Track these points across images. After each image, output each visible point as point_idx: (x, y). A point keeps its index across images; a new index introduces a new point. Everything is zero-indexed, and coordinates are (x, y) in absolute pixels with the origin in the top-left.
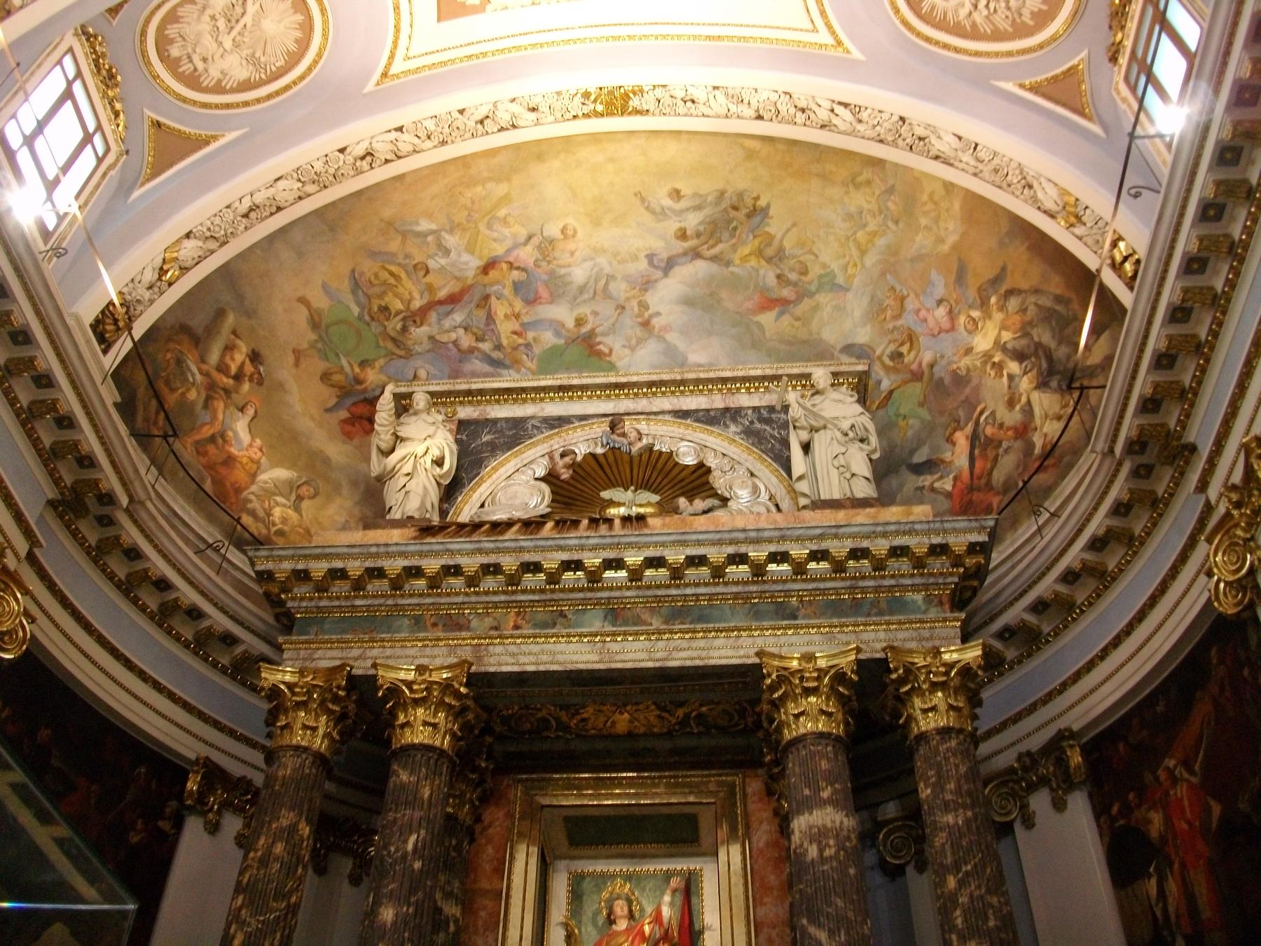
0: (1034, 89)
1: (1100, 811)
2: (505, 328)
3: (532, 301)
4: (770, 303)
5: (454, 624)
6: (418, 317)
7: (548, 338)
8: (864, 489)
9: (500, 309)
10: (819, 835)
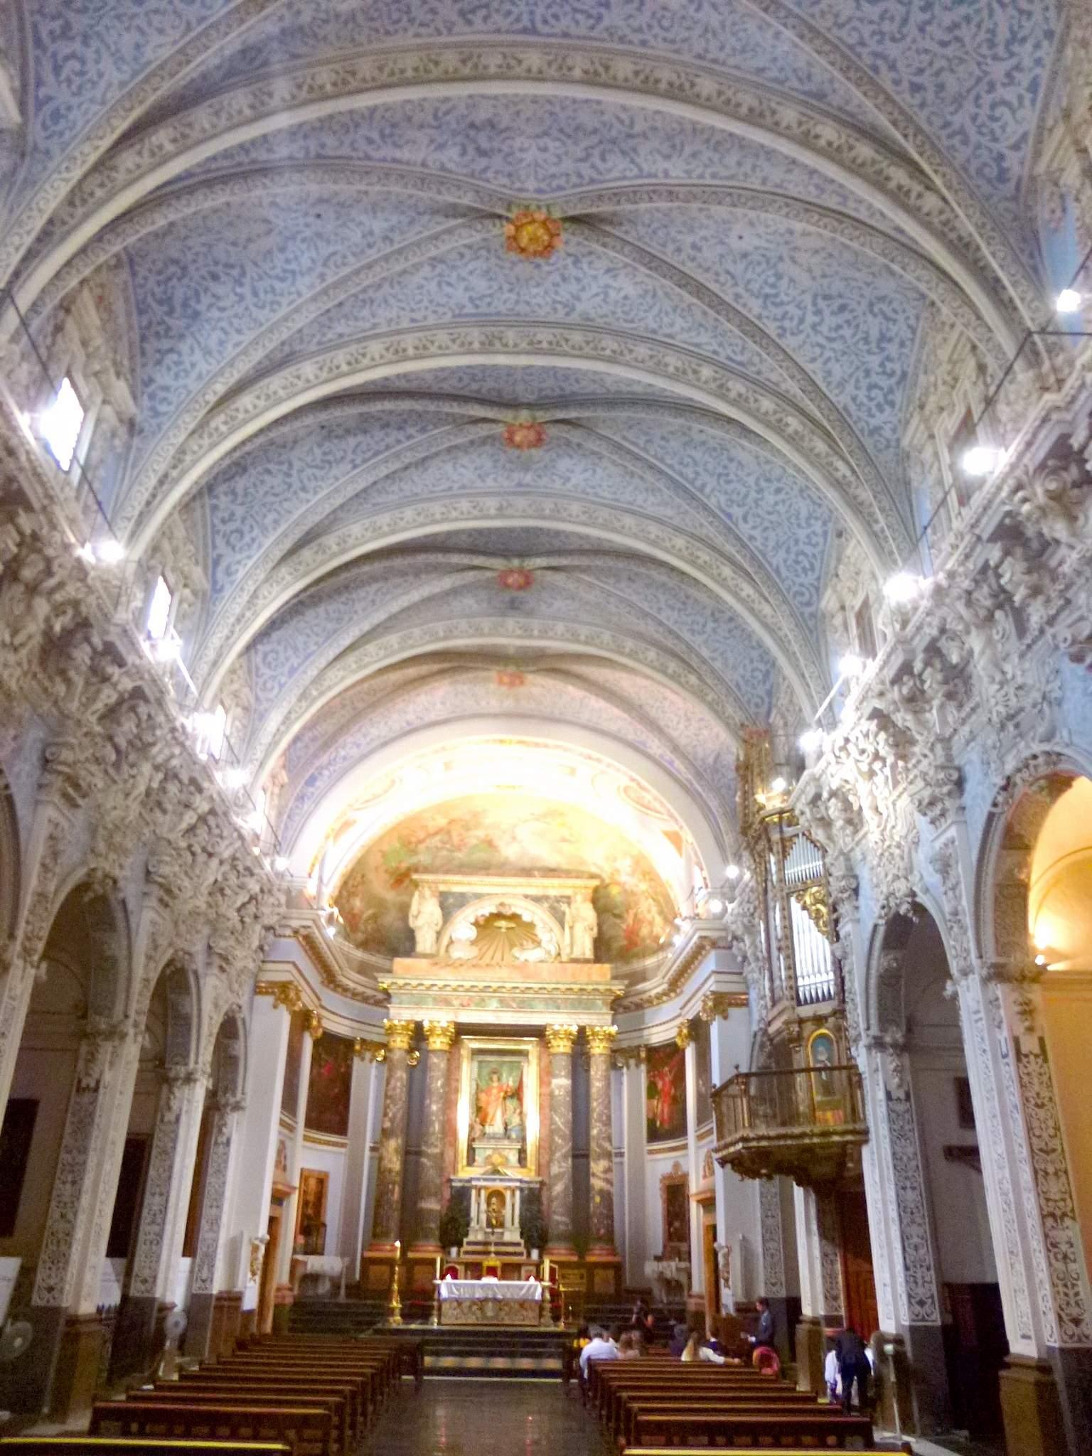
0: (667, 834)
1: (648, 1072)
2: (456, 839)
3: (468, 829)
4: (564, 840)
5: (447, 1002)
6: (420, 842)
7: (474, 841)
8: (589, 954)
9: (454, 834)
10: (560, 1087)
